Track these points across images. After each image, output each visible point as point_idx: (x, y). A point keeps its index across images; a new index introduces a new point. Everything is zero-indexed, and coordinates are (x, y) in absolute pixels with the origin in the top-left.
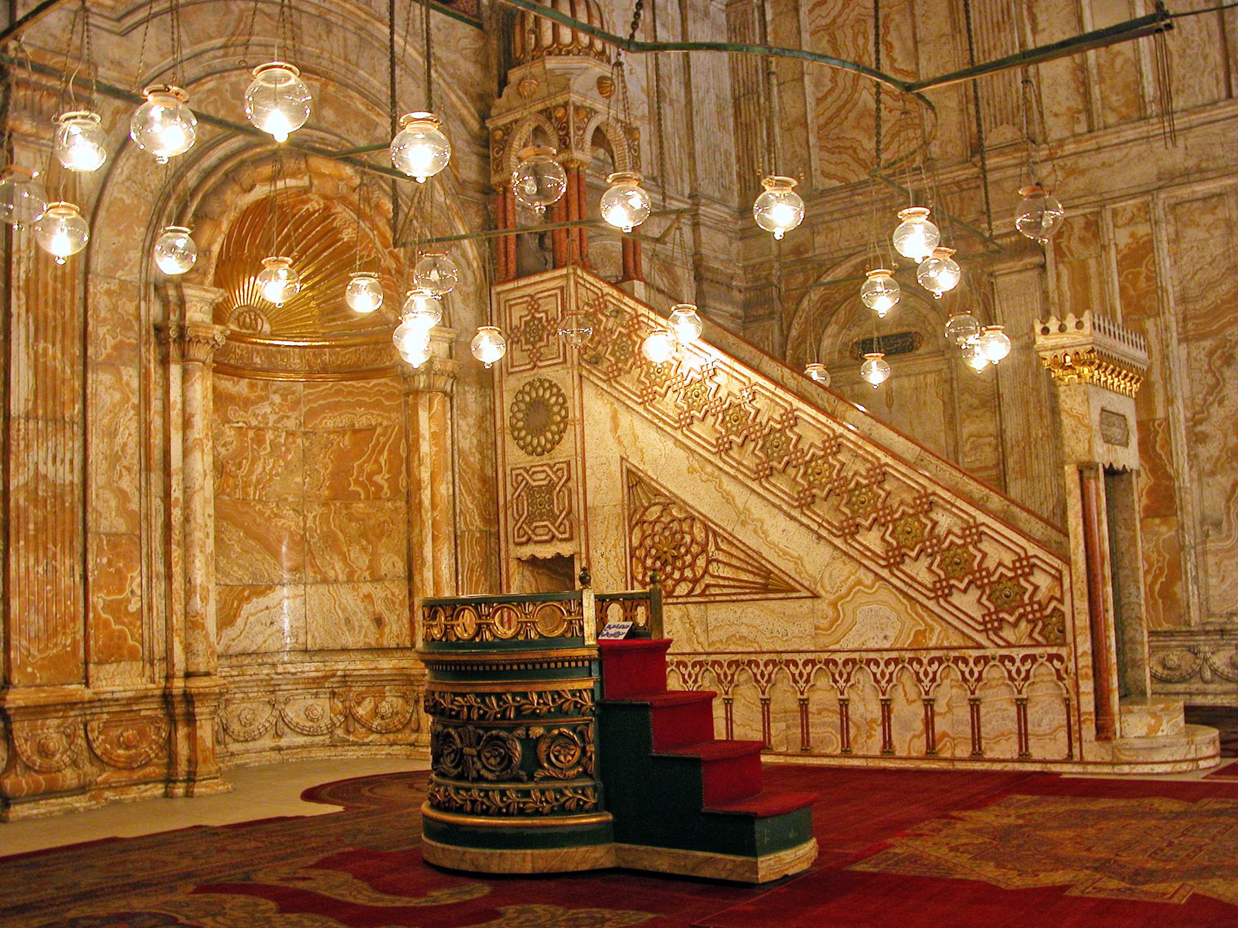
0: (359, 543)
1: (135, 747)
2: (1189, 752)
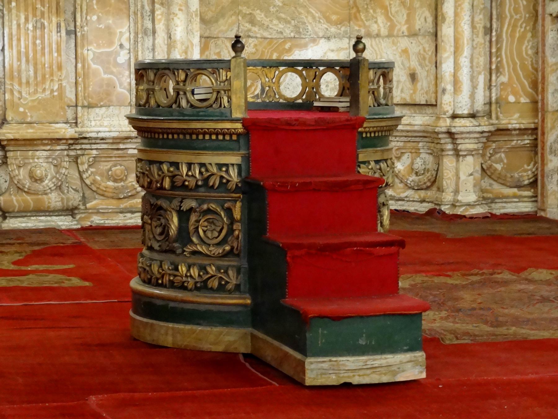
1: (121, 180)
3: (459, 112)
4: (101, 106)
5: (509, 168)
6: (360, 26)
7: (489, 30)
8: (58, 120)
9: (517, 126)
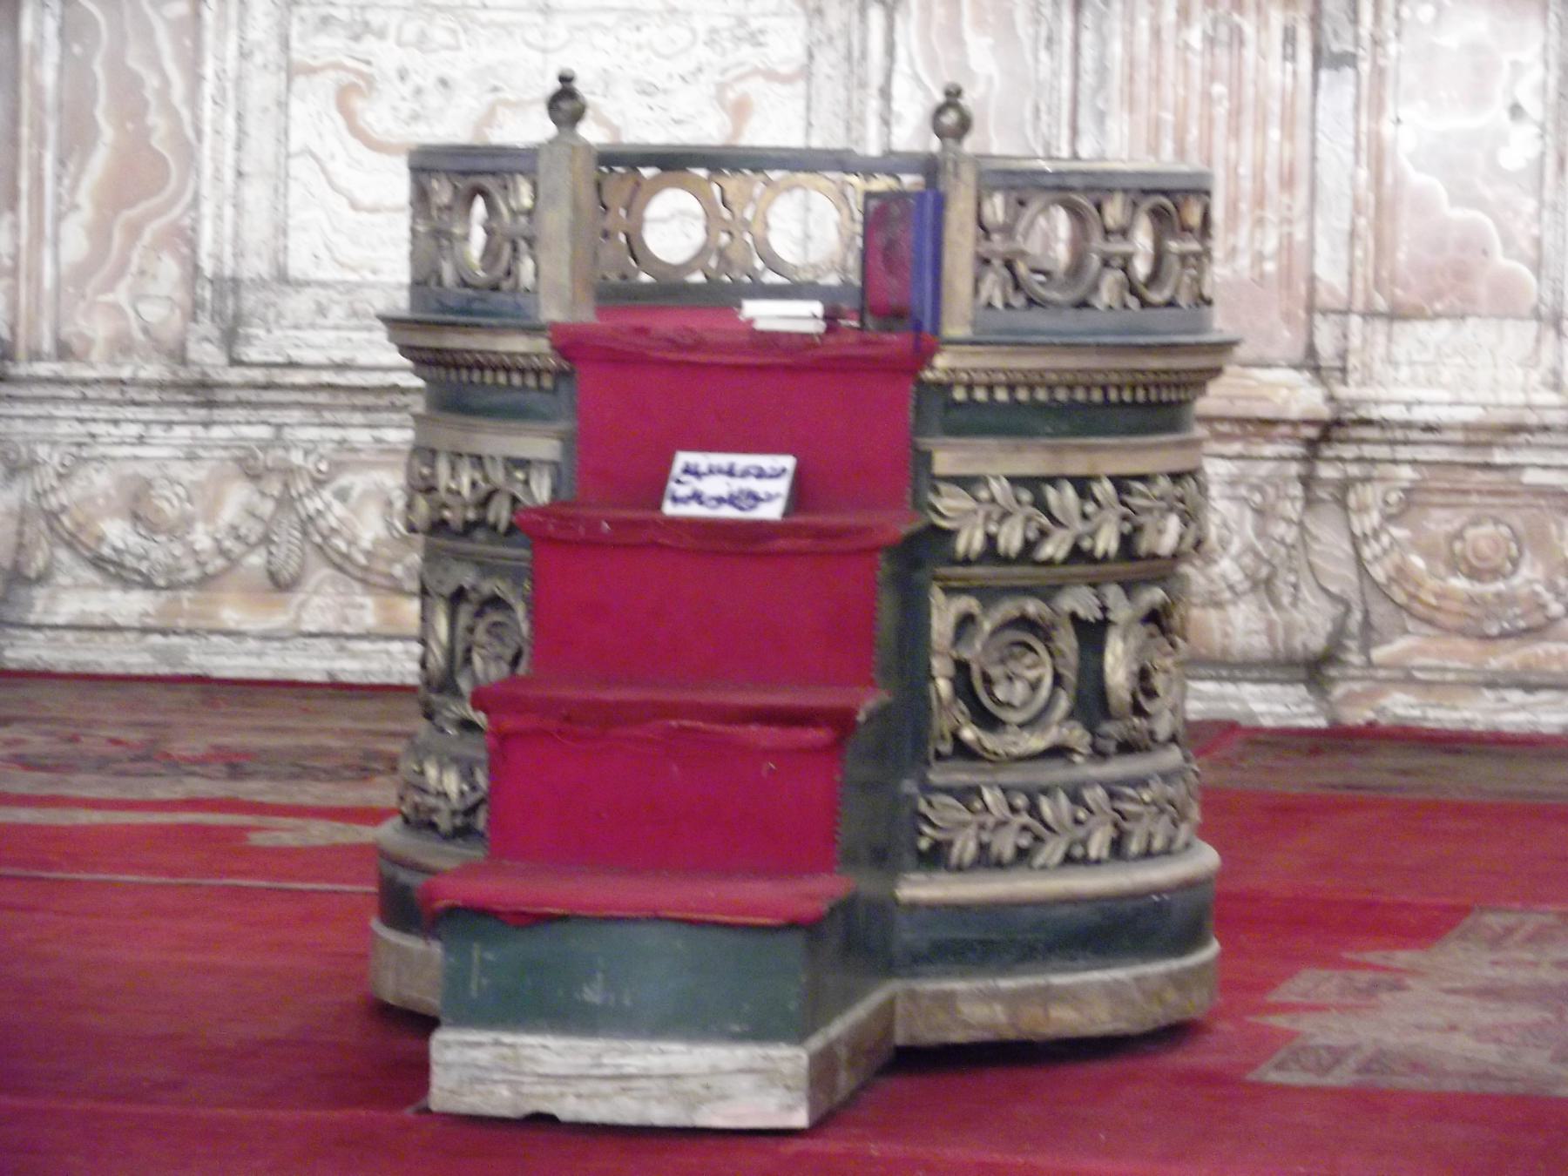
4: (1437, 316)
8: (1272, 353)
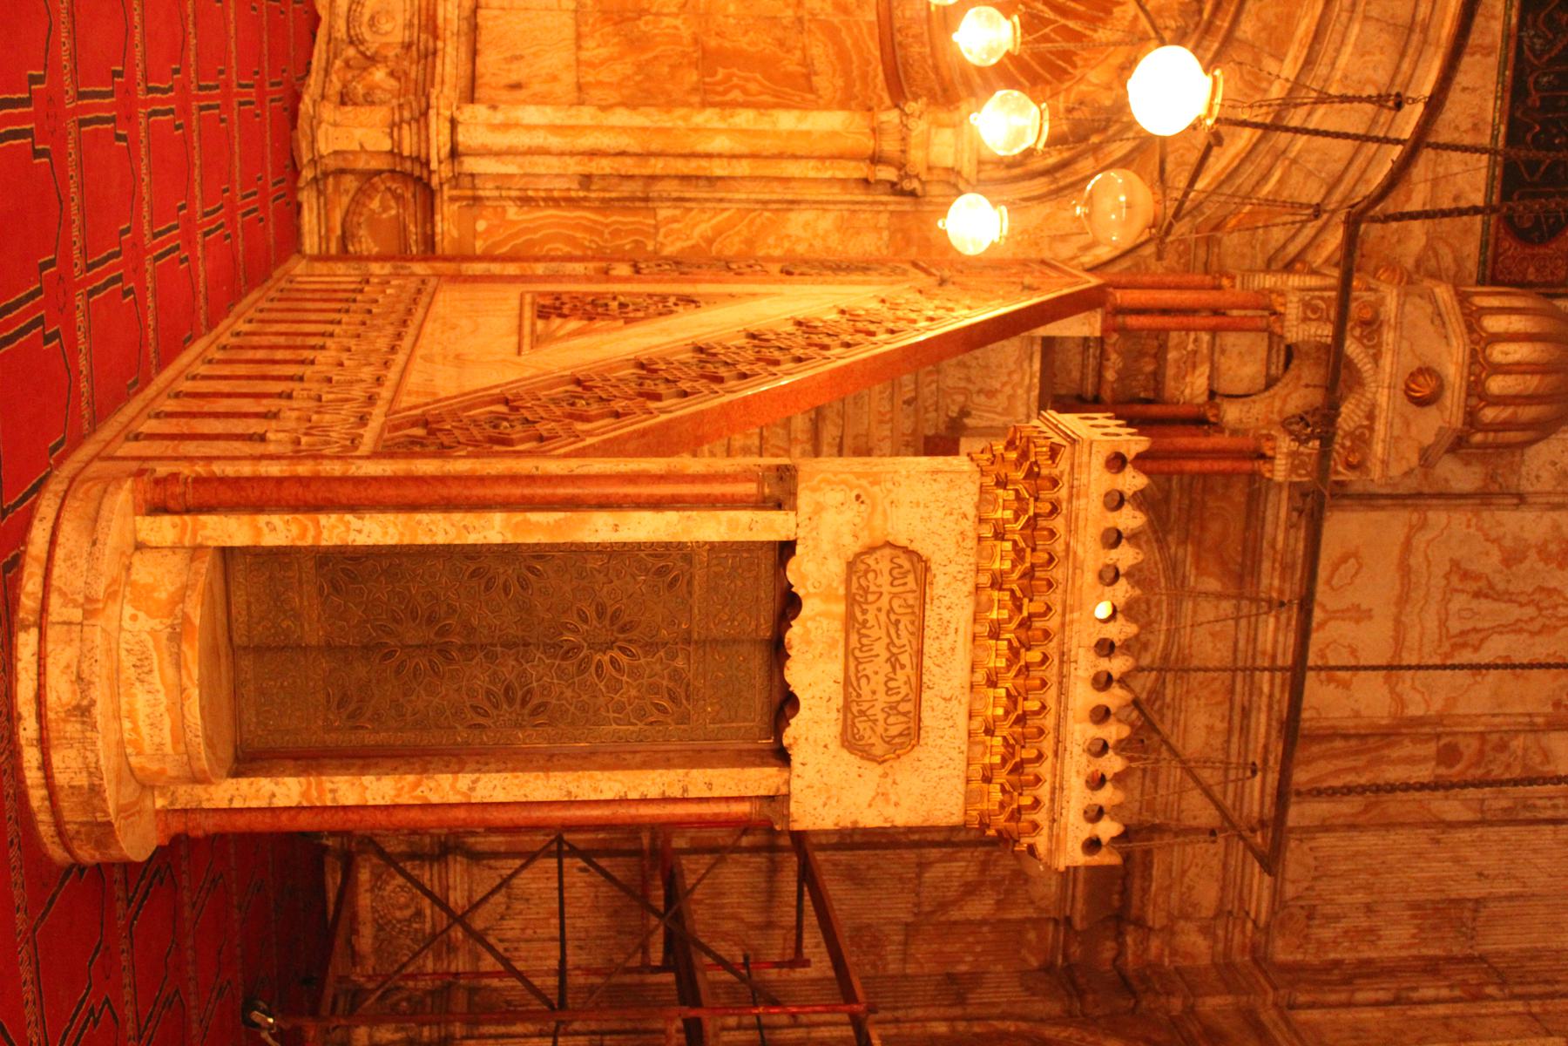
0: (636, 73)
2: (68, 601)
3: (460, 129)
5: (374, 222)
6: (593, 25)
7: (586, 180)
9: (438, 230)
